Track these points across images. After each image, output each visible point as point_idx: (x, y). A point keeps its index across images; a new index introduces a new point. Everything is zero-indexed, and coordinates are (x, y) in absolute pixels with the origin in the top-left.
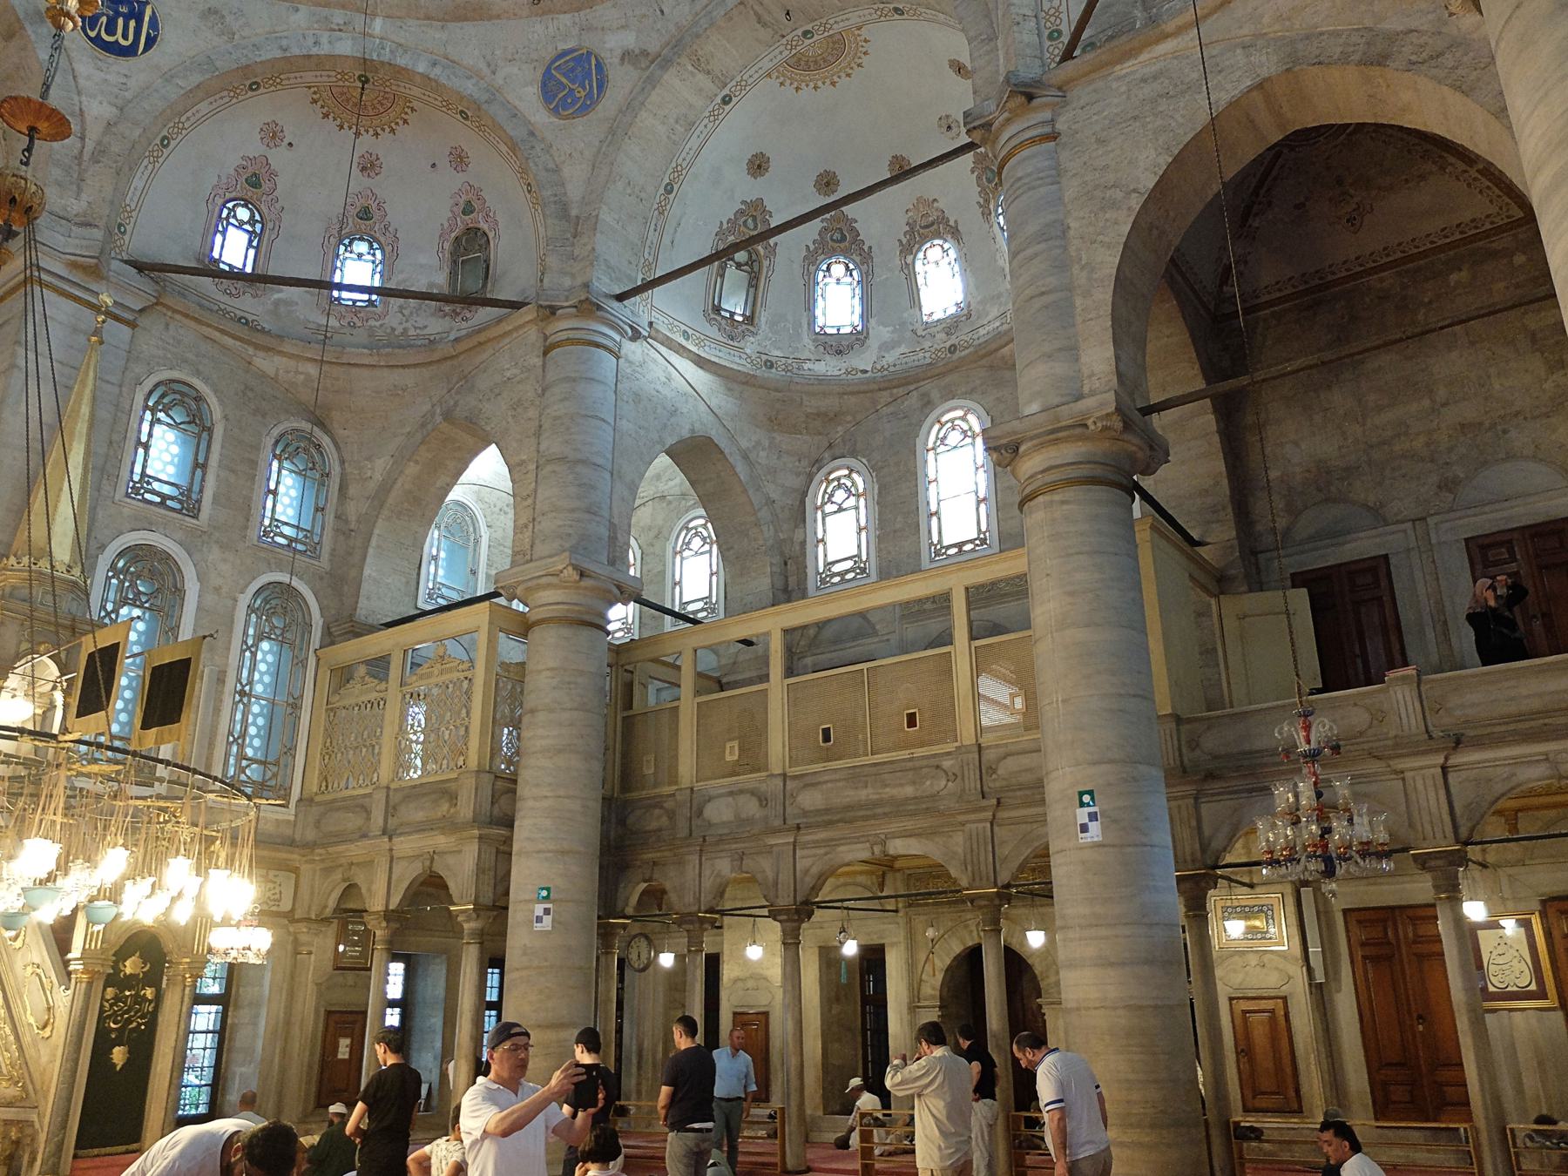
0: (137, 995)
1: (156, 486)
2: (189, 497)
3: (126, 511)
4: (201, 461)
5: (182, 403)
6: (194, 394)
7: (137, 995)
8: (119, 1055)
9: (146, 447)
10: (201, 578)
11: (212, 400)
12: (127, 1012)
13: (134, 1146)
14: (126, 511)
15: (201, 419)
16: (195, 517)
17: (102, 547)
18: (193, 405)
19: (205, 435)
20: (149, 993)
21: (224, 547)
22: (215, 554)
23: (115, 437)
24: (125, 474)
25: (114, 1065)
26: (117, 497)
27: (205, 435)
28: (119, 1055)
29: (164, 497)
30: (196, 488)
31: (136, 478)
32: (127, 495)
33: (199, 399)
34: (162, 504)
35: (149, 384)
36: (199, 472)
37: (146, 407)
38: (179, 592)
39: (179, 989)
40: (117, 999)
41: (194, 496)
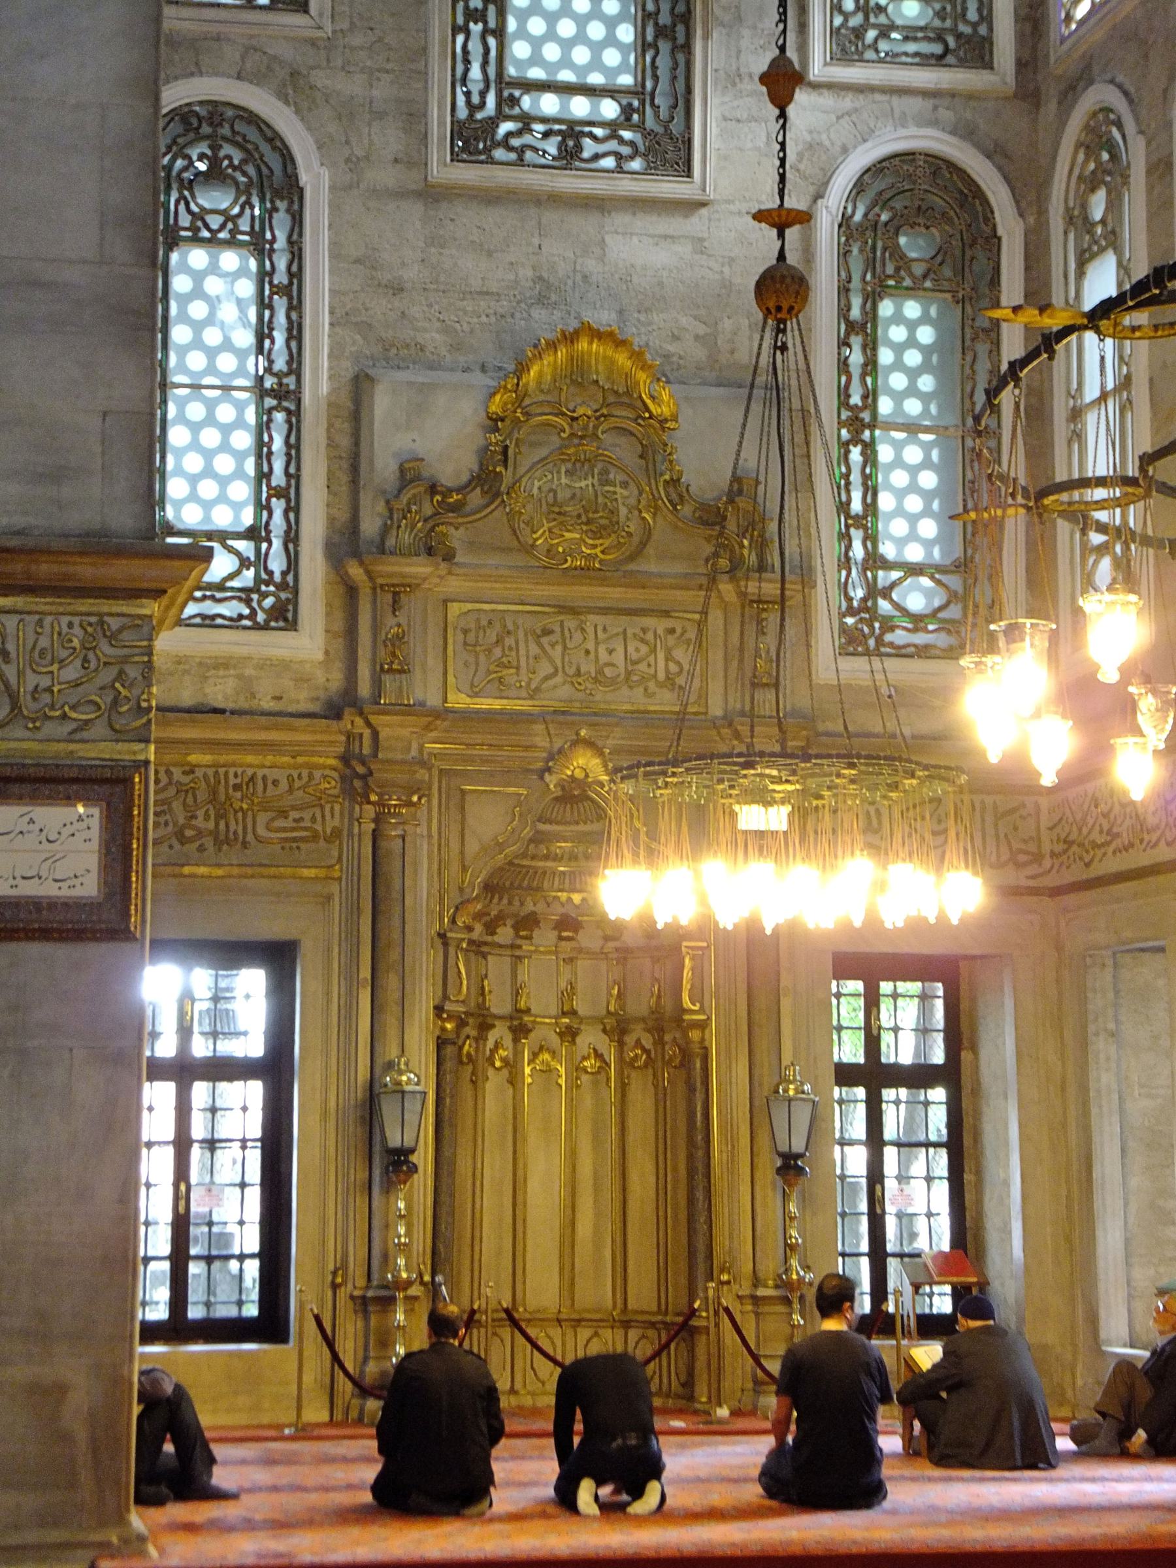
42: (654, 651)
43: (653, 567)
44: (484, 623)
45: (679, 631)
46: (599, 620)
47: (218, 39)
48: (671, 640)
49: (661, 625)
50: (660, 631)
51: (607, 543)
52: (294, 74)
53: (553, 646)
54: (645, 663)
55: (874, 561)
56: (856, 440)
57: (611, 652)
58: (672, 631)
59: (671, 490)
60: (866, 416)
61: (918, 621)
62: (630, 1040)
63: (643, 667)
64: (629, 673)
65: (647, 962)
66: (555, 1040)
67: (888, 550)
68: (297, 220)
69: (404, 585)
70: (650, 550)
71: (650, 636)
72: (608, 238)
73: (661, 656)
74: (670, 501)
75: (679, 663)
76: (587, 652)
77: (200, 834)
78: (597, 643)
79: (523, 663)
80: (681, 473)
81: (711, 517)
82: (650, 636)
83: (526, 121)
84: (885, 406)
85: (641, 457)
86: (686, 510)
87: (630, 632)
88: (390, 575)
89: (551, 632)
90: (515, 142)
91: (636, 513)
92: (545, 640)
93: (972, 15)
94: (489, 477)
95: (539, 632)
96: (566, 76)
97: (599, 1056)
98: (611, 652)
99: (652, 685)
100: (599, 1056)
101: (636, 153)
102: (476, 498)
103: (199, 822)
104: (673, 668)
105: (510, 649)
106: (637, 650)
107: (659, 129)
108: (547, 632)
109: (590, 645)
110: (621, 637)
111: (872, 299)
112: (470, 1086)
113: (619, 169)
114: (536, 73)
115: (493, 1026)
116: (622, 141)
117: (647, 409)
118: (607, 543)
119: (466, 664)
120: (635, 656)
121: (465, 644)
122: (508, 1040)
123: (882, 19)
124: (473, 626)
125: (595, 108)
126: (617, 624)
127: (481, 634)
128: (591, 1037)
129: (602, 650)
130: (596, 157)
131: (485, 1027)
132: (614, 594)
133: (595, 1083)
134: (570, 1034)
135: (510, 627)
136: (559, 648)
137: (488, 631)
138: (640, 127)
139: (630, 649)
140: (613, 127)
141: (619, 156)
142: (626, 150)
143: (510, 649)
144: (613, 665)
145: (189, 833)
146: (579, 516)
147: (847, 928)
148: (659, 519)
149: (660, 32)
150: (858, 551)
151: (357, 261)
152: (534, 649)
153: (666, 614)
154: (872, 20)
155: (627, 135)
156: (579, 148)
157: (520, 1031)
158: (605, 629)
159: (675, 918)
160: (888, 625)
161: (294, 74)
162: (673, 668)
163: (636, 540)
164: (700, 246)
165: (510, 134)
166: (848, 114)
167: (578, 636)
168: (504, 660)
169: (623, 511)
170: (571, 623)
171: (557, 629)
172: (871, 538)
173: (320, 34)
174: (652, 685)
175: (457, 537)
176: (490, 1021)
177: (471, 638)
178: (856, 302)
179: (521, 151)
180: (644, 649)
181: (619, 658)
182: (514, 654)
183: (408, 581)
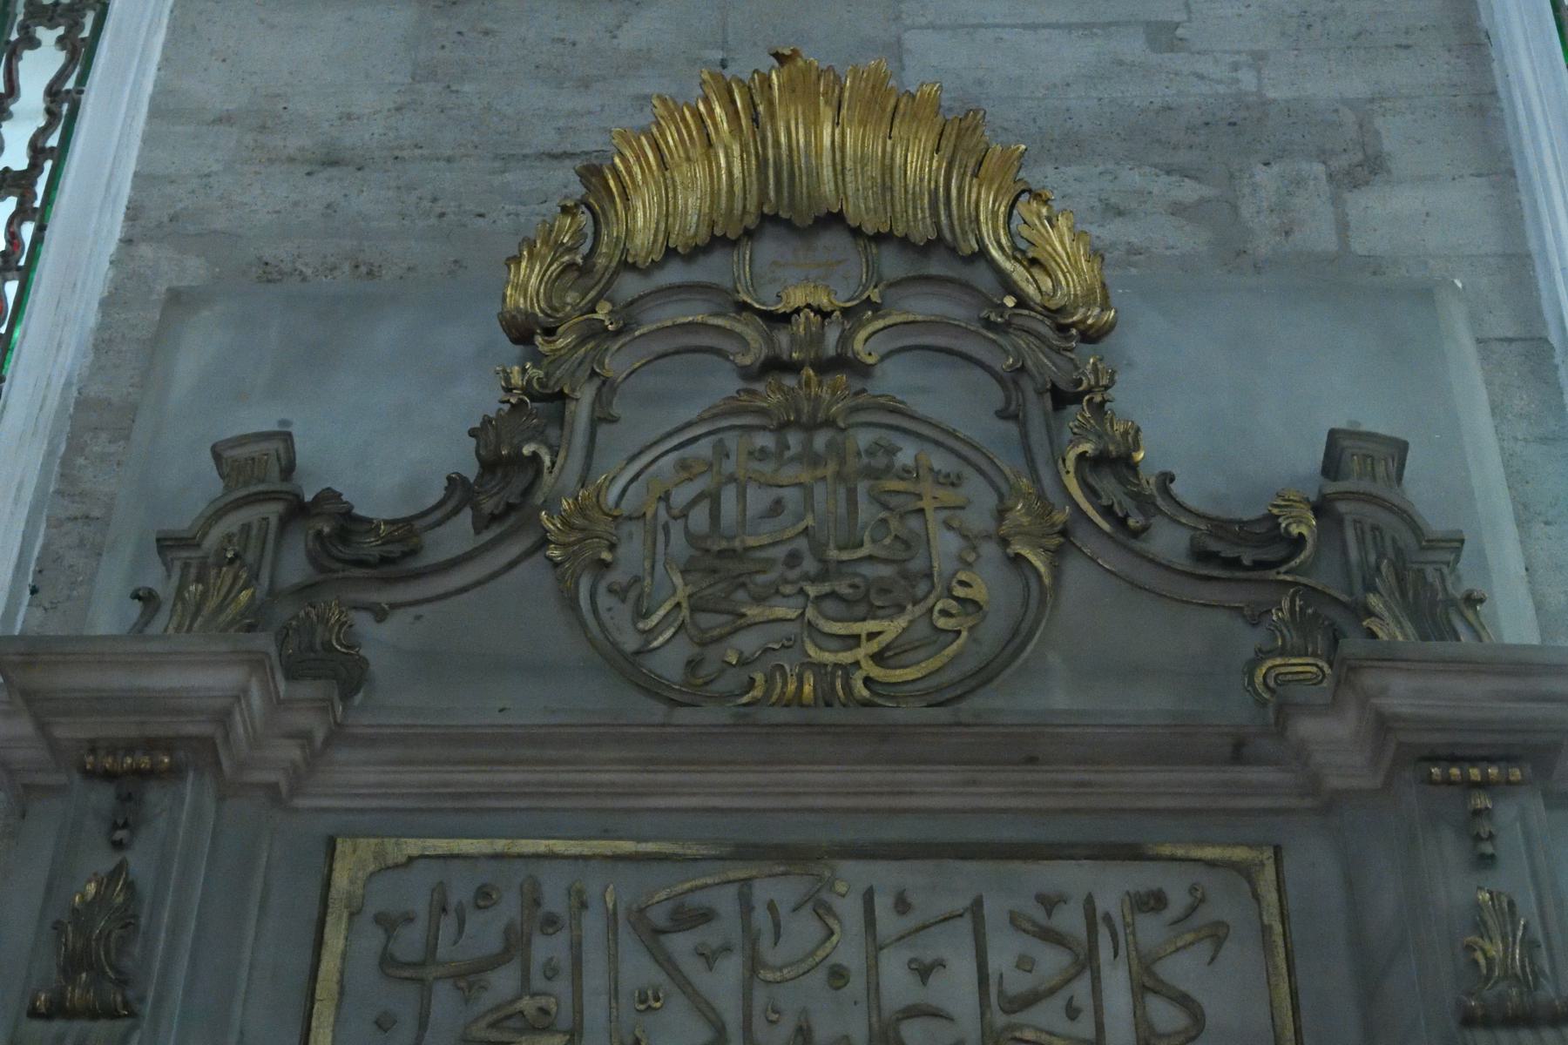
42: (1087, 962)
43: (1060, 698)
44: (461, 892)
45: (1178, 900)
46: (886, 876)
48: (1151, 929)
49: (1112, 886)
50: (1109, 902)
51: (891, 628)
53: (708, 958)
54: (1059, 1001)
57: (924, 972)
58: (1153, 902)
59: (1108, 486)
63: (1048, 1015)
68: (80, 53)
69: (151, 745)
71: (1070, 920)
72: (912, 39)
74: (1108, 512)
75: (1184, 1001)
76: (838, 976)
78: (875, 947)
79: (595, 1010)
80: (1133, 438)
81: (1242, 554)
82: (1070, 920)
85: (1003, 415)
86: (1169, 541)
87: (995, 910)
88: (99, 703)
89: (706, 916)
91: (990, 550)
92: (681, 944)
94: (500, 485)
95: (659, 916)
98: (924, 972)
102: (459, 534)
104: (1166, 1017)
105: (551, 972)
106: (1025, 963)
108: (690, 917)
109: (850, 954)
110: (965, 925)
117: (1009, 286)
118: (891, 628)
119: (384, 1024)
120: (1018, 983)
121: (387, 962)
124: (421, 907)
126: (944, 888)
127: (448, 925)
129: (894, 968)
132: (937, 792)
135: (555, 901)
136: (731, 969)
137: (474, 920)
139: (1001, 961)
143: (551, 972)
144: (936, 1014)
146: (793, 559)
148: (1075, 570)
152: (639, 969)
153: (1132, 853)
158: (902, 905)
163: (995, 628)
167: (803, 930)
168: (527, 1004)
169: (945, 545)
170: (778, 889)
171: (725, 902)
175: (381, 640)
177: (410, 942)
180: (1052, 961)
181: (956, 988)
182: (562, 986)
183: (159, 727)
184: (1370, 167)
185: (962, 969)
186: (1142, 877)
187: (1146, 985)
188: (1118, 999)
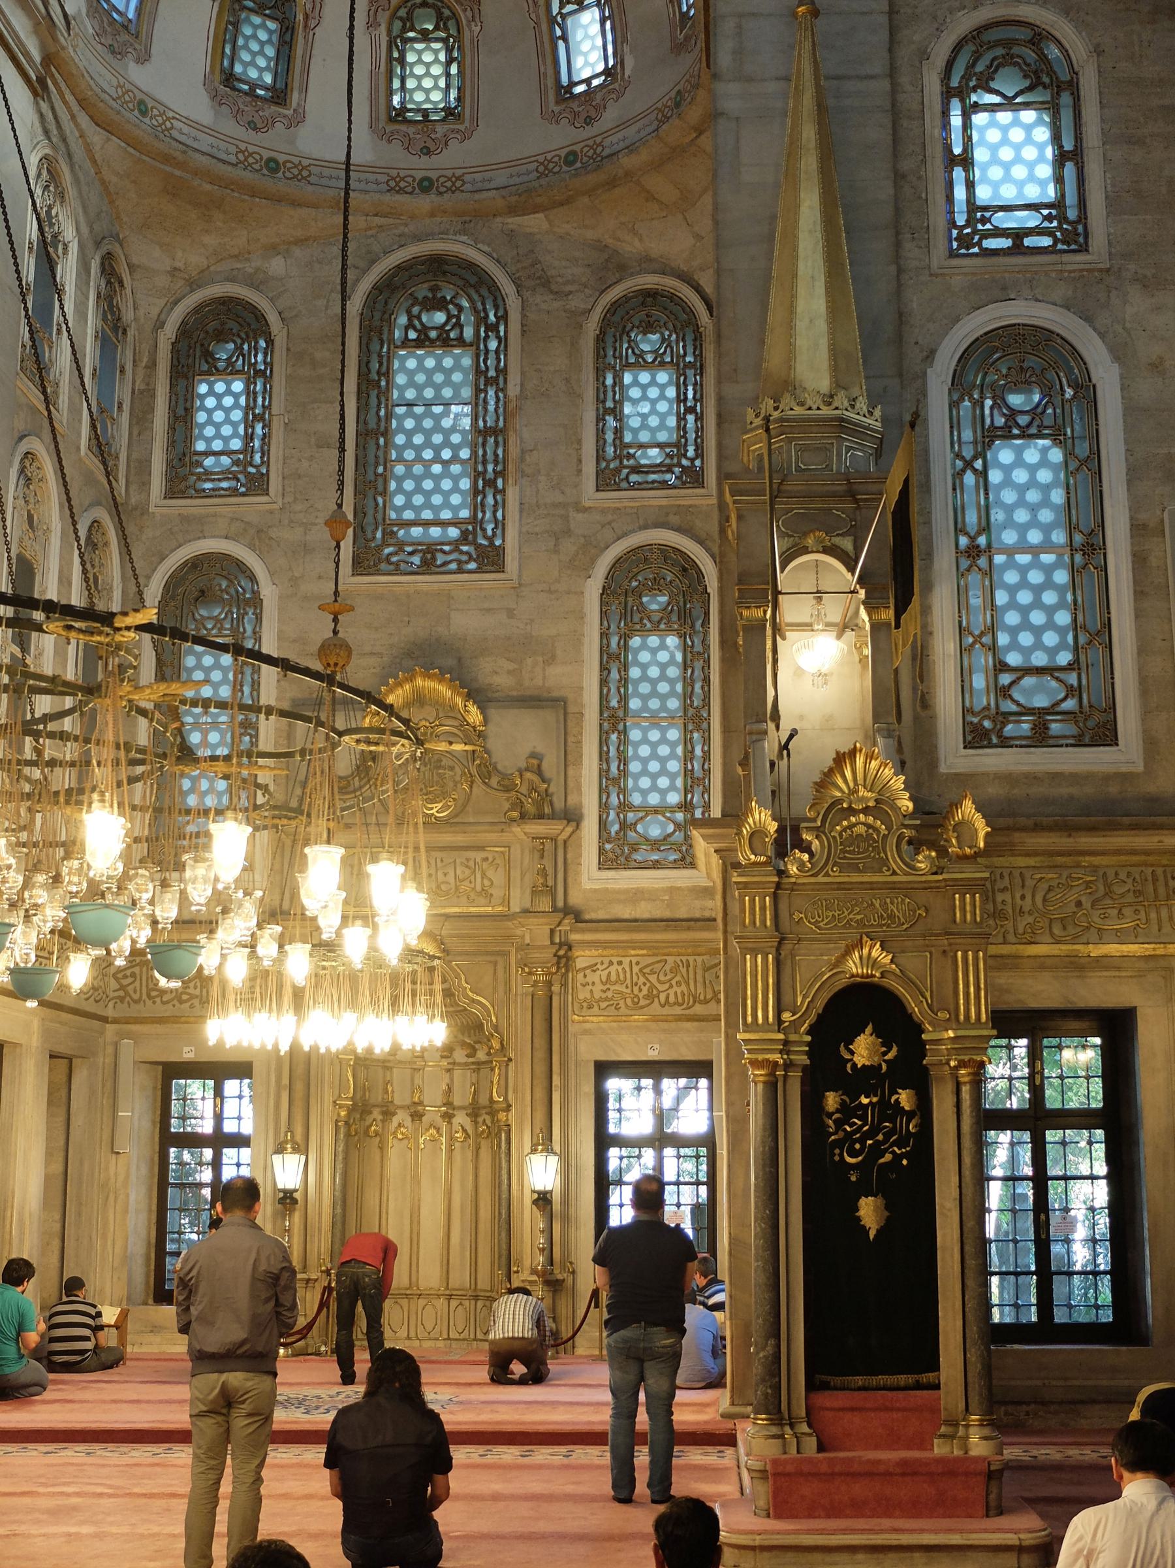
0: (884, 1104)
1: (1002, 220)
2: (1062, 218)
3: (957, 281)
4: (1068, 145)
5: (1008, 60)
6: (1023, 34)
7: (884, 1104)
8: (869, 1211)
9: (966, 161)
10: (1119, 353)
11: (1064, 29)
12: (871, 1134)
13: (929, 1377)
14: (957, 281)
15: (1051, 73)
16: (1084, 249)
17: (930, 356)
18: (1031, 55)
19: (1066, 99)
20: (905, 1098)
21: (1144, 284)
22: (1136, 304)
23: (906, 165)
24: (938, 220)
25: (865, 1231)
26: (935, 264)
27: (1066, 99)
28: (869, 1211)
29: (1018, 235)
30: (1071, 199)
31: (961, 220)
32: (953, 254)
33: (1039, 37)
34: (1018, 248)
35: (941, 52)
36: (1069, 169)
37: (948, 94)
38: (1087, 392)
39: (950, 1087)
40: (847, 1111)
41: (1072, 214)
47: (215, 515)
48: (485, 865)
49: (479, 856)
52: (259, 531)
55: (625, 806)
56: (614, 729)
60: (621, 713)
61: (655, 844)
62: (480, 1120)
64: (457, 888)
65: (380, 1070)
66: (439, 1120)
67: (636, 799)
68: (259, 619)
70: (469, 809)
71: (471, 863)
72: (453, 614)
73: (479, 876)
77: (192, 997)
83: (400, 546)
84: (634, 704)
90: (394, 559)
93: (691, 452)
96: (427, 515)
97: (464, 1130)
99: (472, 895)
100: (464, 1130)
101: (471, 558)
103: (191, 991)
104: (486, 883)
107: (485, 543)
111: (625, 637)
112: (377, 1151)
113: (460, 571)
114: (408, 515)
115: (394, 1114)
116: (462, 552)
122: (408, 1121)
123: (632, 462)
125: (445, 532)
128: (461, 1119)
130: (445, 564)
131: (388, 1114)
133: (462, 1148)
134: (448, 1117)
138: (474, 543)
140: (456, 543)
141: (459, 562)
142: (464, 558)
145: (185, 997)
147: (250, 1047)
149: (487, 483)
150: (614, 800)
151: (294, 641)
153: (481, 848)
154: (625, 462)
155: (465, 548)
156: (434, 558)
157: (417, 1116)
159: (350, 1043)
160: (634, 848)
161: (259, 531)
162: (486, 883)
164: (510, 613)
165: (391, 554)
166: (609, 523)
172: (623, 791)
173: (275, 506)
174: (472, 895)
176: (392, 1109)
178: (614, 641)
179: (397, 564)
180: (467, 872)
184: (551, 660)
185: (452, 874)
186: (483, 855)
187: (484, 875)
188: (479, 880)
